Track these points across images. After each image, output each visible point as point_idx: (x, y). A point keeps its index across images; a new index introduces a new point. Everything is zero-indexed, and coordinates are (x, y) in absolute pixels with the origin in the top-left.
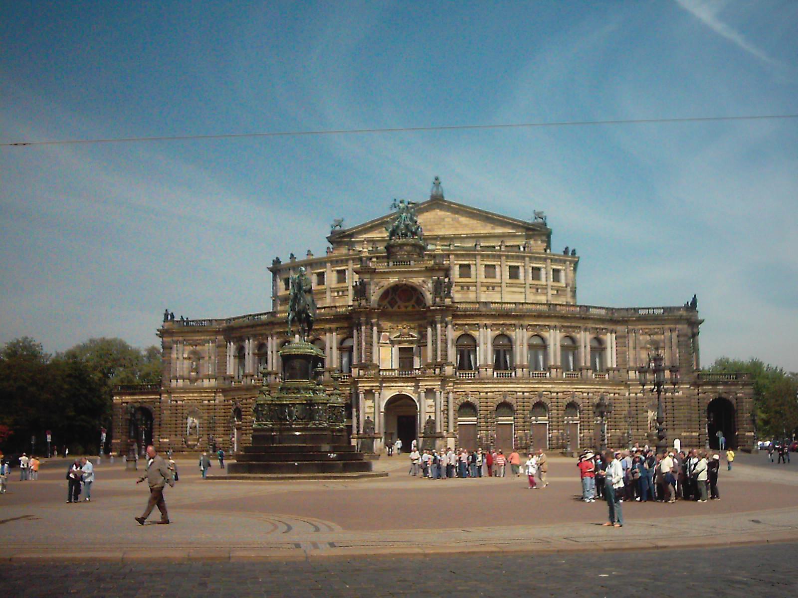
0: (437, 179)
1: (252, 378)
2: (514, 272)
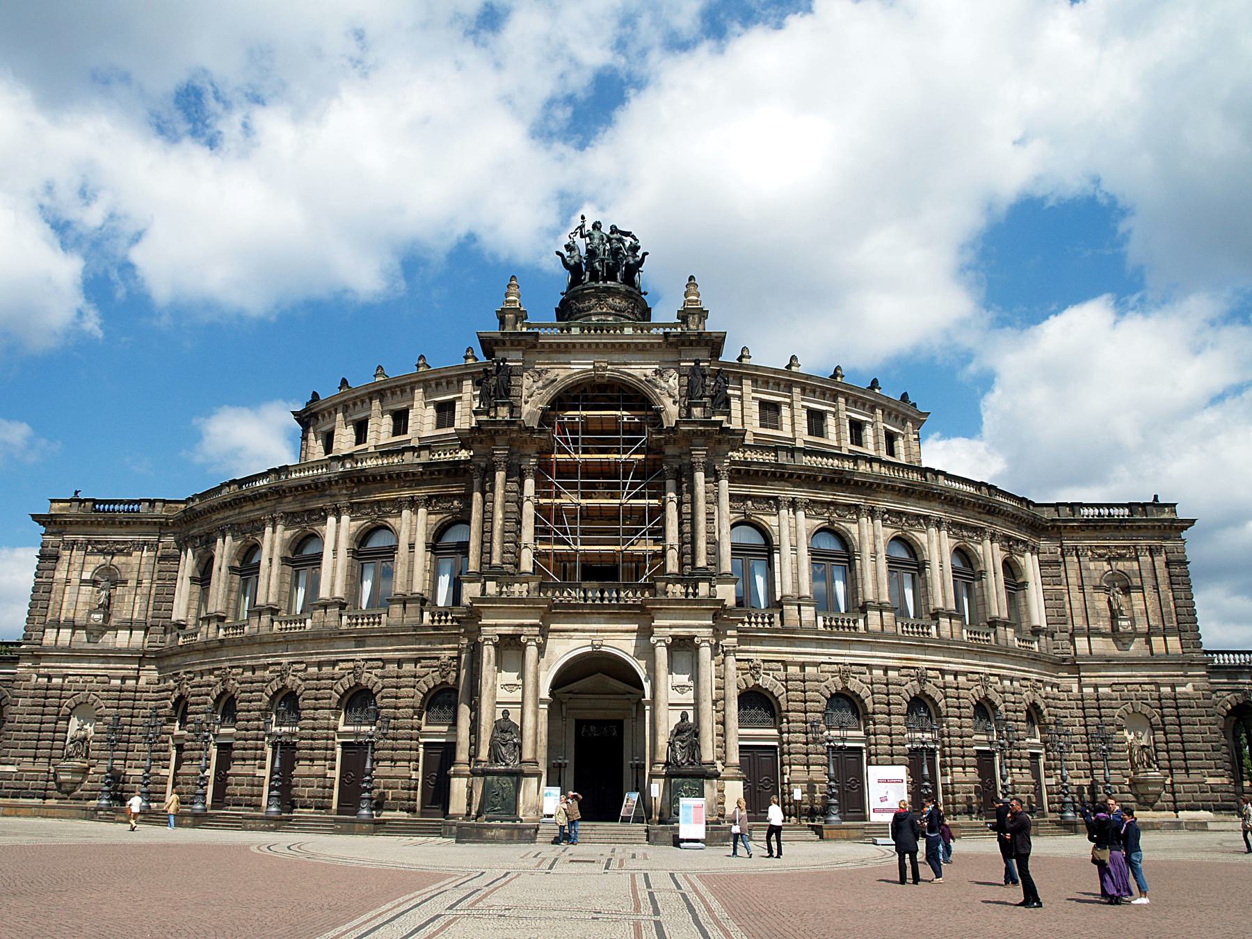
1: (221, 624)
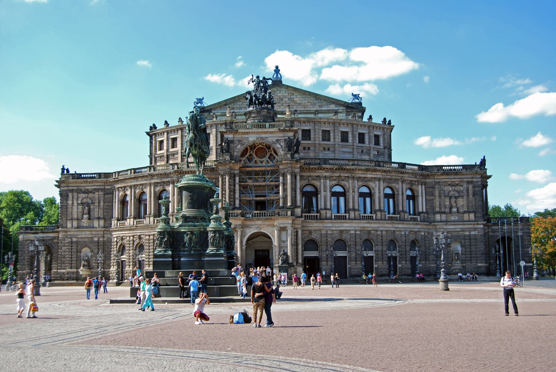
0: (277, 67)
2: (344, 137)
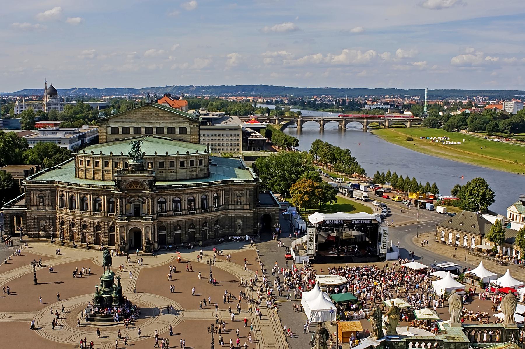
2: (182, 164)
